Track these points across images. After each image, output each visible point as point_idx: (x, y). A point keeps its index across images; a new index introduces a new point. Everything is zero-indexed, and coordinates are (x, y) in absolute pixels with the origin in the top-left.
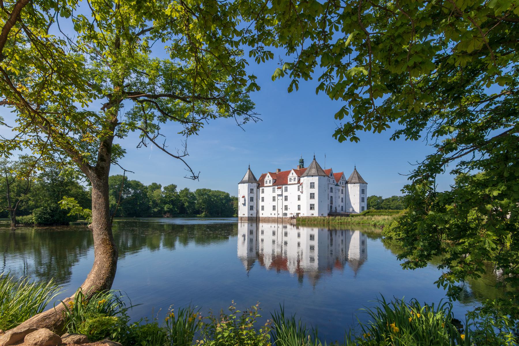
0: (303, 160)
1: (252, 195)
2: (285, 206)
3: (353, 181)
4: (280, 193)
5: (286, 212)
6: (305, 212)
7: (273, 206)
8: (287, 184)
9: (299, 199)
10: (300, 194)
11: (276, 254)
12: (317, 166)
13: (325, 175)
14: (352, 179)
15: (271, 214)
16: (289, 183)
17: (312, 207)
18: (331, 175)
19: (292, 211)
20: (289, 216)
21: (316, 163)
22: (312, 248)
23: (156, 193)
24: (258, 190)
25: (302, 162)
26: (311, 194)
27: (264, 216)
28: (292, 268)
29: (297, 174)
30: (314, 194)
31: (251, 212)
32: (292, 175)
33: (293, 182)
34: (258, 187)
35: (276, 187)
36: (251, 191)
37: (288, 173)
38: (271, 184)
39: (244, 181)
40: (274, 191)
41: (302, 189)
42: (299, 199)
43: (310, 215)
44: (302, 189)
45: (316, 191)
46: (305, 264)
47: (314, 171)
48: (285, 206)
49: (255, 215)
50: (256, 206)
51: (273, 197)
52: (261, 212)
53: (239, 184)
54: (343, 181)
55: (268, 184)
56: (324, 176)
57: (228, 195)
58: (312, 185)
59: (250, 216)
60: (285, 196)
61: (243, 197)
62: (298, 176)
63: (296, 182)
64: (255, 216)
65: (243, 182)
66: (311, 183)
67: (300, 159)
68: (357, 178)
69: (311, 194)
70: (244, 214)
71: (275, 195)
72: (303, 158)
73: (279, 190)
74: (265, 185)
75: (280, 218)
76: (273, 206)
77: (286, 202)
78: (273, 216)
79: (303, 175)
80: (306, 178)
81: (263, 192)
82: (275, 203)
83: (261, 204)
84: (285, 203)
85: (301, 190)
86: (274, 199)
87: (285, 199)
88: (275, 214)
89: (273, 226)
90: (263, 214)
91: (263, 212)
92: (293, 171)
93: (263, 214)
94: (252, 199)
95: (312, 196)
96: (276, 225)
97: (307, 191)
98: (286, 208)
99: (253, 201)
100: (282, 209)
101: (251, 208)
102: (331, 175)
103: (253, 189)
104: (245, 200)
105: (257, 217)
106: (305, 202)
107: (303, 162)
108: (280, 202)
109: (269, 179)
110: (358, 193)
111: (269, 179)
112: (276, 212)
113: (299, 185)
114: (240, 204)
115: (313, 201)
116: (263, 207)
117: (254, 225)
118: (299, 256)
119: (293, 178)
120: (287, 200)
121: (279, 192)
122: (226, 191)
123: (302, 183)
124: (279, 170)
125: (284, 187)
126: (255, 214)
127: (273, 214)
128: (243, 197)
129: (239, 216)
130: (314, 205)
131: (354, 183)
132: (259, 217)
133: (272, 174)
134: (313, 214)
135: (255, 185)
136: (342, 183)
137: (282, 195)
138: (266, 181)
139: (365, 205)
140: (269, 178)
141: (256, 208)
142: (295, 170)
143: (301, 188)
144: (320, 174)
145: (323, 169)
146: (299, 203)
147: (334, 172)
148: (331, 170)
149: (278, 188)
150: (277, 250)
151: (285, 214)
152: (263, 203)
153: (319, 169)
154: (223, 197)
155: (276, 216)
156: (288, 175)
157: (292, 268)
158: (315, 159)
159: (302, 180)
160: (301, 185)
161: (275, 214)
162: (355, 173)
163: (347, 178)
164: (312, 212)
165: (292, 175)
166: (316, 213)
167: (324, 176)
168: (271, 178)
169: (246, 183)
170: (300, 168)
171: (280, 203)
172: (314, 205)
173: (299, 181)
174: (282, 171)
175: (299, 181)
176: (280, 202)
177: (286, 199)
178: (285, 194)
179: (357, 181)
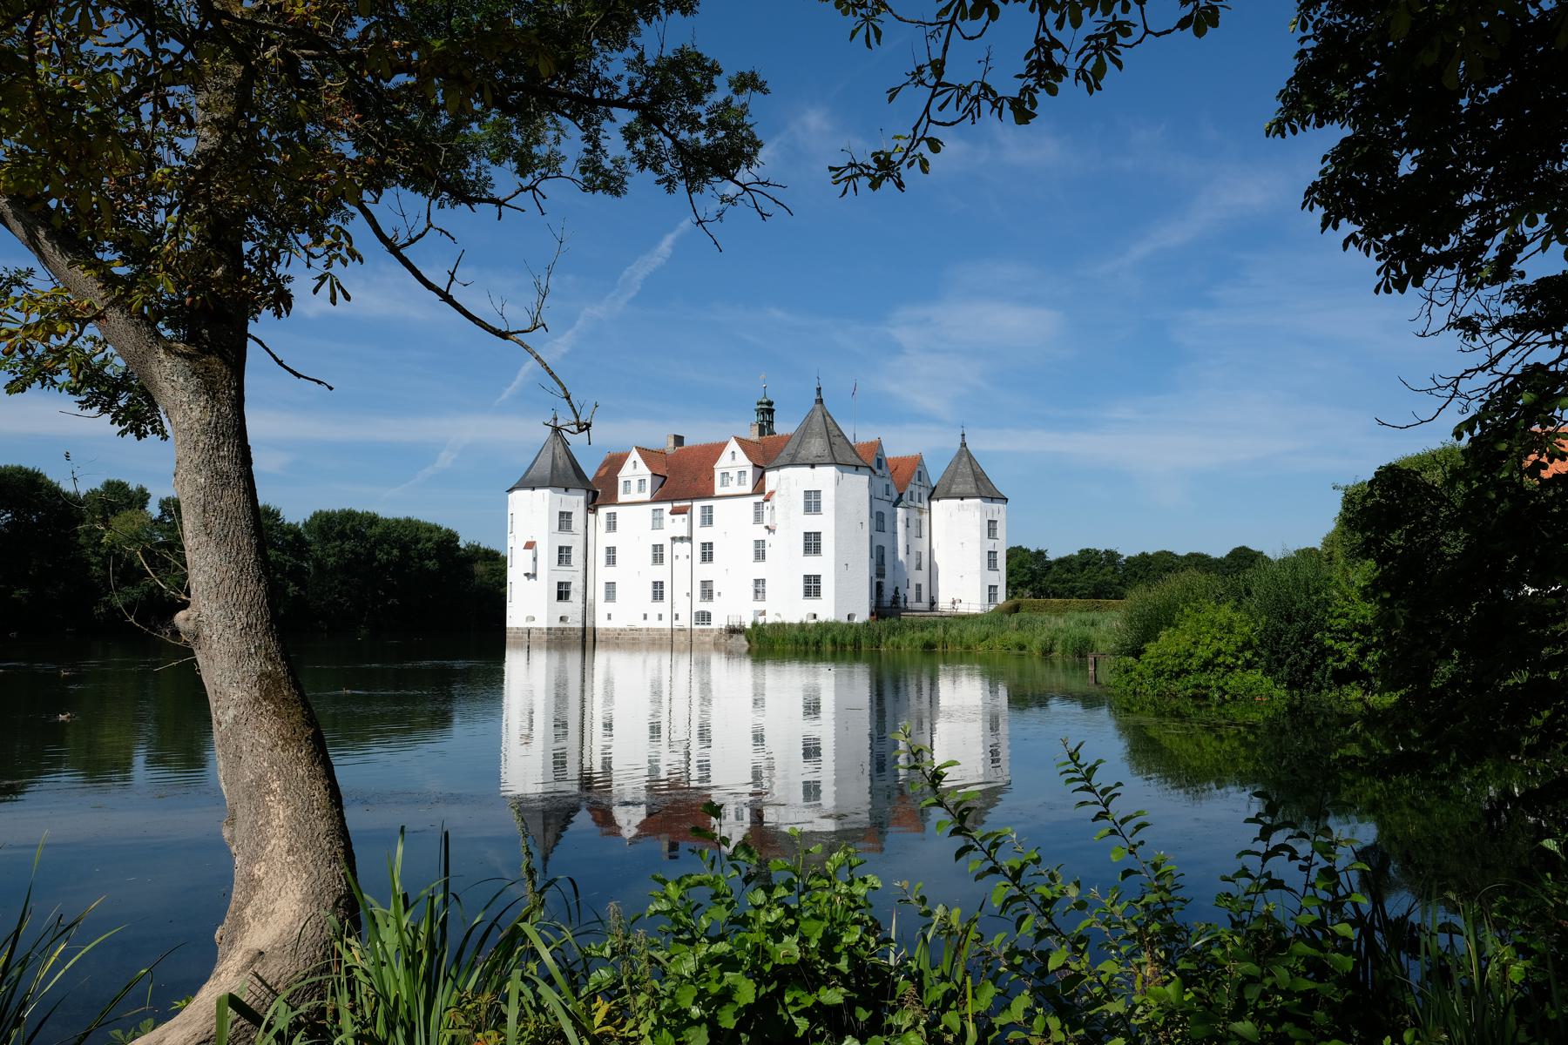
0: (770, 403)
1: (565, 539)
3: (955, 489)
4: (685, 534)
6: (789, 608)
7: (655, 583)
8: (711, 496)
9: (760, 555)
10: (759, 532)
12: (831, 427)
13: (860, 463)
14: (952, 480)
15: (645, 617)
16: (718, 491)
17: (812, 586)
18: (880, 467)
19: (736, 608)
20: (719, 622)
21: (826, 415)
22: (811, 751)
23: (122, 525)
24: (591, 516)
26: (807, 535)
27: (617, 624)
28: (733, 828)
29: (749, 457)
30: (818, 535)
31: (563, 608)
32: (733, 464)
33: (733, 488)
34: (592, 506)
35: (667, 507)
36: (565, 519)
37: (716, 451)
38: (647, 496)
39: (532, 481)
40: (657, 522)
41: (772, 518)
42: (760, 555)
44: (772, 518)
46: (789, 815)
47: (817, 446)
50: (581, 584)
52: (602, 609)
53: (511, 490)
54: (922, 489)
55: (635, 496)
56: (857, 467)
57: (452, 538)
58: (812, 502)
59: (557, 624)
61: (530, 545)
62: (755, 466)
63: (748, 488)
64: (580, 625)
65: (528, 483)
68: (971, 479)
69: (807, 535)
71: (662, 537)
73: (679, 518)
74: (622, 498)
77: (707, 566)
78: (653, 623)
79: (778, 462)
81: (612, 525)
82: (660, 573)
83: (602, 573)
84: (704, 571)
85: (767, 522)
86: (658, 555)
87: (704, 555)
88: (660, 617)
89: (657, 663)
90: (609, 617)
91: (610, 607)
92: (733, 445)
93: (609, 617)
94: (564, 554)
95: (812, 543)
96: (666, 658)
97: (791, 521)
98: (707, 591)
99: (568, 563)
100: (690, 595)
101: (563, 593)
102: (880, 467)
103: (569, 514)
104: (535, 559)
105: (584, 629)
106: (788, 566)
107: (771, 412)
108: (682, 566)
109: (635, 473)
110: (978, 534)
111: (635, 473)
113: (760, 499)
114: (514, 575)
115: (813, 565)
116: (610, 588)
117: (574, 659)
118: (757, 775)
119: (734, 473)
120: (711, 559)
121: (678, 526)
122: (445, 524)
123: (772, 493)
124: (679, 440)
125: (697, 506)
126: (580, 618)
127: (657, 618)
128: (530, 545)
130: (817, 578)
131: (962, 499)
132: (594, 629)
133: (648, 455)
134: (815, 616)
135: (575, 502)
136: (916, 497)
137: (690, 539)
138: (627, 483)
139: (1000, 578)
140: (637, 471)
141: (581, 590)
142: (740, 442)
143: (767, 513)
144: (839, 460)
145: (851, 441)
146: (760, 570)
147: (891, 453)
148: (879, 445)
149: (673, 512)
150: (669, 762)
151: (705, 617)
152: (611, 569)
153: (838, 441)
154: (430, 545)
155: (665, 624)
157: (733, 828)
158: (821, 401)
159: (771, 477)
160: (767, 500)
161: (660, 617)
162: (965, 459)
163: (935, 475)
164: (812, 605)
165: (733, 464)
166: (826, 609)
167: (857, 467)
168: (644, 472)
169: (543, 487)
170: (761, 433)
171: (683, 572)
172: (817, 578)
173: (759, 488)
174: (687, 443)
175: (759, 488)
176: (682, 566)
177: (707, 553)
178: (701, 535)
179: (970, 487)
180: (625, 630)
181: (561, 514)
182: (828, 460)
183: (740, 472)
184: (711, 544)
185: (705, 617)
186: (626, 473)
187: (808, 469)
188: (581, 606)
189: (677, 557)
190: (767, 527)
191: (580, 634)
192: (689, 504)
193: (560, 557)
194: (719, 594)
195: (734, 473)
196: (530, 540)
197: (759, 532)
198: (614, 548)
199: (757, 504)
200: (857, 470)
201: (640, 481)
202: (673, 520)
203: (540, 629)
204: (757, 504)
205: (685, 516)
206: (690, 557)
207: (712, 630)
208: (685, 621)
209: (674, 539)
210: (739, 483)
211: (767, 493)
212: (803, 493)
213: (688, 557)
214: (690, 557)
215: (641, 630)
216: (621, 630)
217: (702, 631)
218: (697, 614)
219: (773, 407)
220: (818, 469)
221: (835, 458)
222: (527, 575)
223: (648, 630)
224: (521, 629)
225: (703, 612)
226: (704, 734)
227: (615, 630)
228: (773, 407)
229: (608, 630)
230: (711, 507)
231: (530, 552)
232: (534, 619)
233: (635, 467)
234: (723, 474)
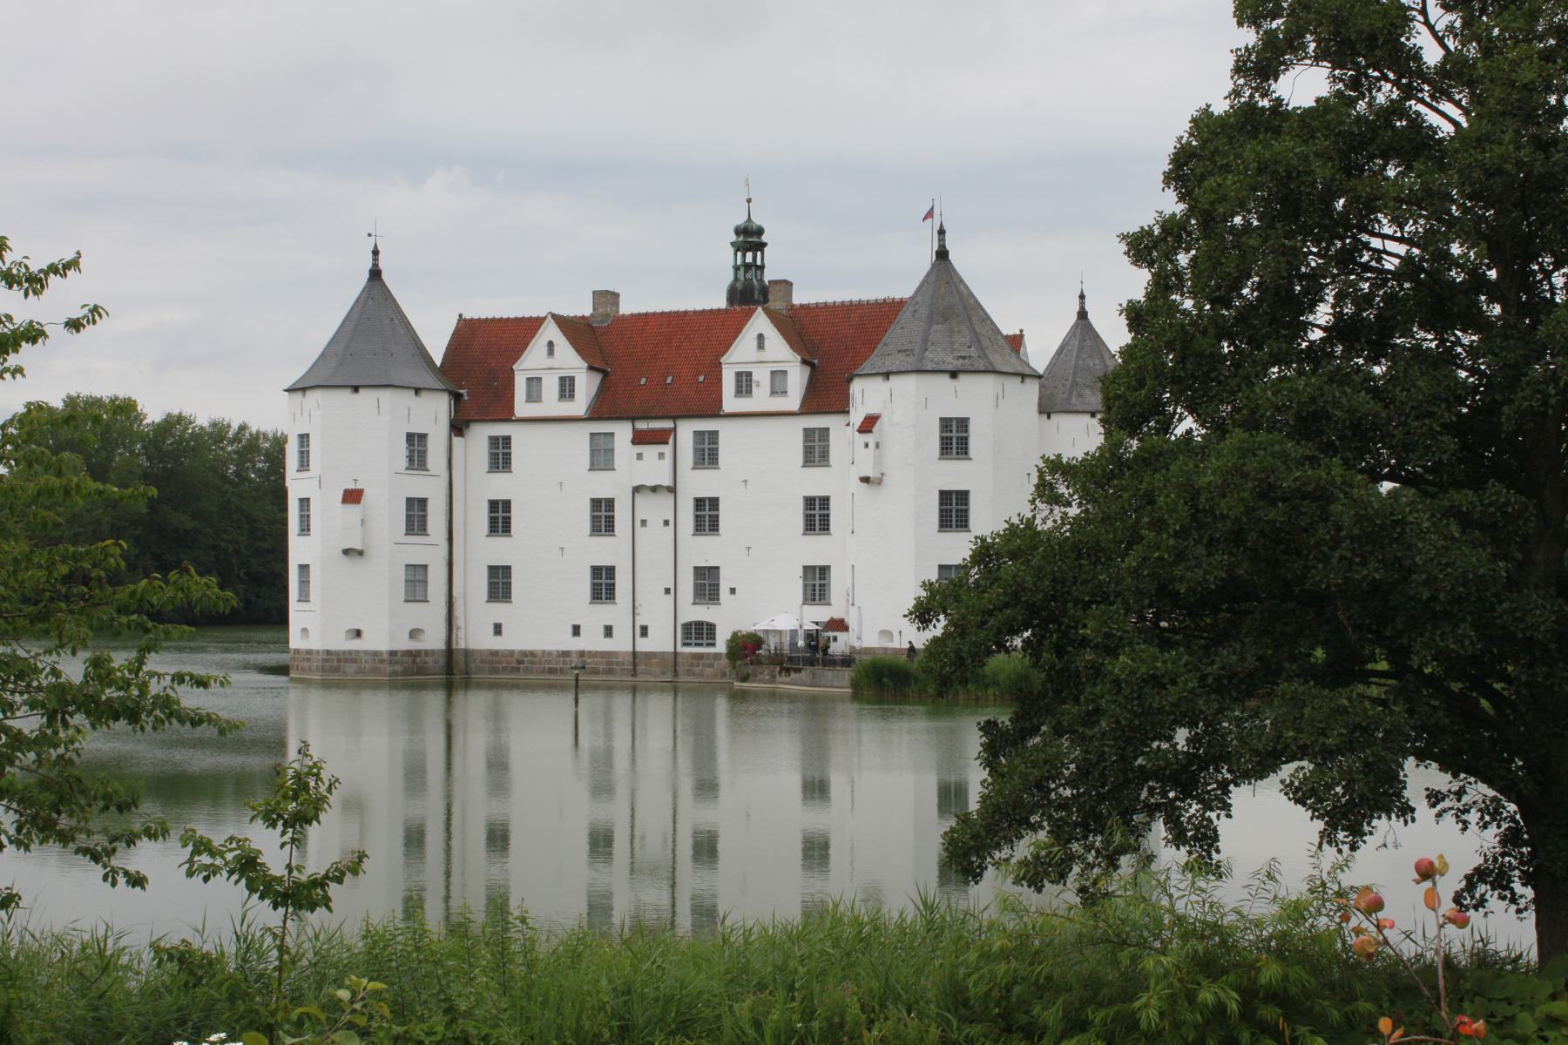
0: (760, 232)
2: (700, 572)
4: (666, 481)
5: (703, 613)
7: (596, 571)
8: (713, 410)
11: (621, 912)
13: (1027, 371)
15: (576, 630)
16: (730, 403)
24: (456, 440)
25: (750, 239)
26: (945, 496)
27: (512, 641)
30: (963, 496)
33: (761, 399)
35: (622, 432)
38: (579, 406)
40: (601, 457)
41: (878, 461)
48: (700, 572)
49: (434, 640)
51: (596, 504)
55: (551, 404)
59: (405, 644)
60: (699, 503)
61: (353, 497)
62: (804, 362)
63: (793, 401)
66: (946, 423)
67: (741, 220)
69: (945, 496)
70: (358, 633)
71: (604, 485)
72: (757, 220)
73: (650, 451)
74: (522, 408)
75: (649, 656)
76: (596, 571)
77: (706, 541)
78: (592, 641)
79: (874, 362)
80: (906, 385)
82: (608, 551)
83: (480, 550)
84: (702, 551)
86: (602, 517)
88: (608, 631)
90: (498, 629)
91: (499, 611)
93: (498, 629)
98: (707, 583)
103: (423, 437)
105: (450, 651)
107: (761, 246)
108: (655, 541)
112: (616, 613)
121: (652, 466)
125: (686, 431)
128: (353, 497)
129: (296, 641)
137: (672, 490)
138: (534, 383)
146: (817, 550)
149: (640, 439)
152: (499, 542)
155: (621, 643)
156: (726, 345)
159: (866, 394)
161: (608, 631)
168: (569, 359)
176: (655, 541)
177: (707, 515)
180: (532, 654)
181: (410, 437)
182: (981, 365)
183: (773, 373)
184: (714, 503)
185: (700, 632)
186: (532, 361)
187: (946, 379)
188: (443, 611)
189: (644, 523)
190: (866, 480)
191: (442, 661)
192: (668, 424)
193: (410, 519)
195: (761, 376)
196: (351, 486)
197: (817, 482)
198: (507, 504)
200: (1022, 382)
201: (562, 379)
202: (639, 456)
203: (376, 654)
204: (809, 433)
205: (667, 449)
207: (717, 656)
208: (661, 640)
209: (637, 490)
210: (773, 393)
211: (857, 416)
212: (937, 423)
213: (666, 523)
214: (671, 523)
215: (566, 654)
216: (524, 654)
217: (700, 656)
218: (687, 627)
219: (764, 238)
220: (962, 378)
221: (991, 364)
222: (346, 552)
223: (582, 654)
224: (337, 653)
225: (699, 624)
226: (706, 849)
227: (512, 653)
228: (764, 238)
229: (494, 653)
230: (714, 435)
231: (353, 509)
232: (358, 633)
233: (551, 352)
234: (739, 374)
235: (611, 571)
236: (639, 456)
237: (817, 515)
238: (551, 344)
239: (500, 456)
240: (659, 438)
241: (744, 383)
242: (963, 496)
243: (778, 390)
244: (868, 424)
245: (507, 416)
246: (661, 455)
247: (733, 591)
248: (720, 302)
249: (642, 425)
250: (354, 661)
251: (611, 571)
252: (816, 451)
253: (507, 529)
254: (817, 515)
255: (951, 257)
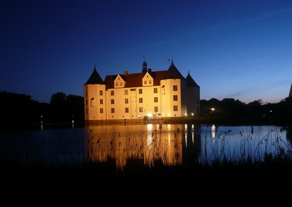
8: (141, 86)
16: (144, 85)
17: (175, 108)
27: (115, 118)
30: (177, 96)
32: (148, 78)
35: (129, 89)
38: (123, 86)
43: (173, 116)
45: (178, 93)
55: (119, 86)
58: (175, 88)
63: (152, 84)
72: (146, 62)
73: (133, 92)
75: (133, 120)
93: (113, 117)
95: (175, 98)
99: (102, 104)
125: (138, 89)
135: (103, 87)
146: (156, 105)
149: (131, 90)
177: (141, 100)
180: (117, 120)
189: (132, 102)
191: (106, 121)
192: (135, 88)
194: (145, 110)
196: (92, 98)
197: (156, 95)
198: (114, 100)
199: (154, 89)
202: (131, 93)
204: (154, 89)
206: (136, 102)
211: (162, 85)
214: (136, 102)
215: (122, 120)
216: (116, 120)
227: (115, 120)
229: (112, 120)
230: (141, 90)
235: (128, 108)
236: (131, 93)
237: (156, 100)
238: (119, 78)
239: (112, 93)
240: (134, 90)
241: (146, 83)
242: (177, 96)
243: (150, 83)
244: (163, 86)
245: (113, 88)
246: (134, 93)
247: (145, 110)
248: (141, 72)
249: (132, 88)
250: (94, 121)
251: (128, 108)
252: (156, 91)
253: (114, 103)
254: (156, 100)
255: (174, 64)
